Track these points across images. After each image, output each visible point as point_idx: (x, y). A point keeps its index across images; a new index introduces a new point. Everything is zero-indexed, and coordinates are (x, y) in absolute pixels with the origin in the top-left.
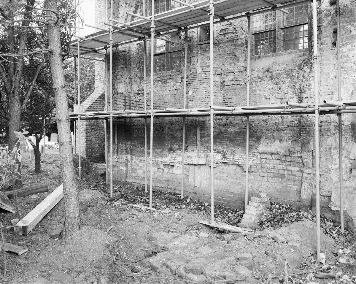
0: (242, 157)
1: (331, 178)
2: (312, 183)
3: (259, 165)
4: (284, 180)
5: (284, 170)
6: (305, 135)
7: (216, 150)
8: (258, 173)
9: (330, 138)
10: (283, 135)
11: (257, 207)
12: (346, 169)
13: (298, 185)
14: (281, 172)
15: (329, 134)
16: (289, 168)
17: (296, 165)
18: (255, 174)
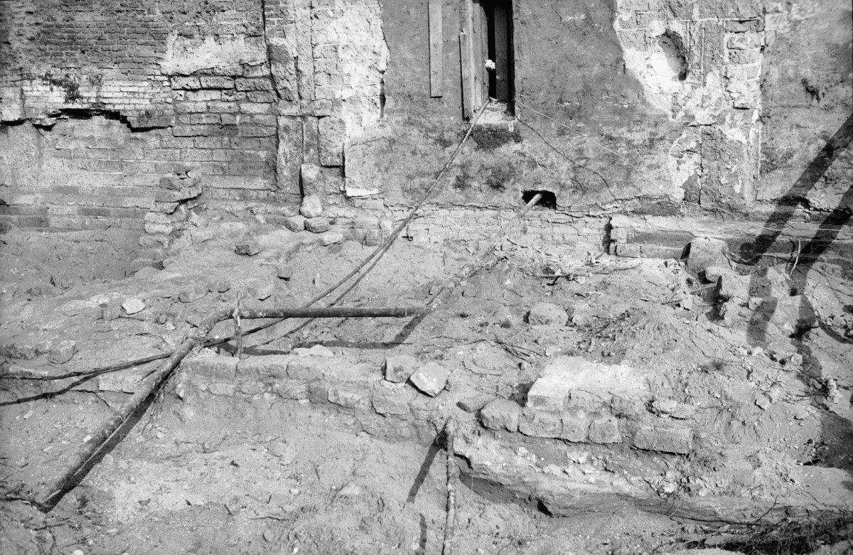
0: (123, 89)
1: (341, 122)
2: (300, 138)
3: (169, 106)
4: (236, 139)
5: (234, 114)
6: (275, 20)
7: (49, 78)
8: (169, 128)
9: (334, 23)
10: (224, 23)
11: (171, 214)
12: (373, 98)
13: (267, 149)
14: (227, 119)
15: (331, 13)
16: (245, 107)
17: (261, 98)
18: (160, 131)
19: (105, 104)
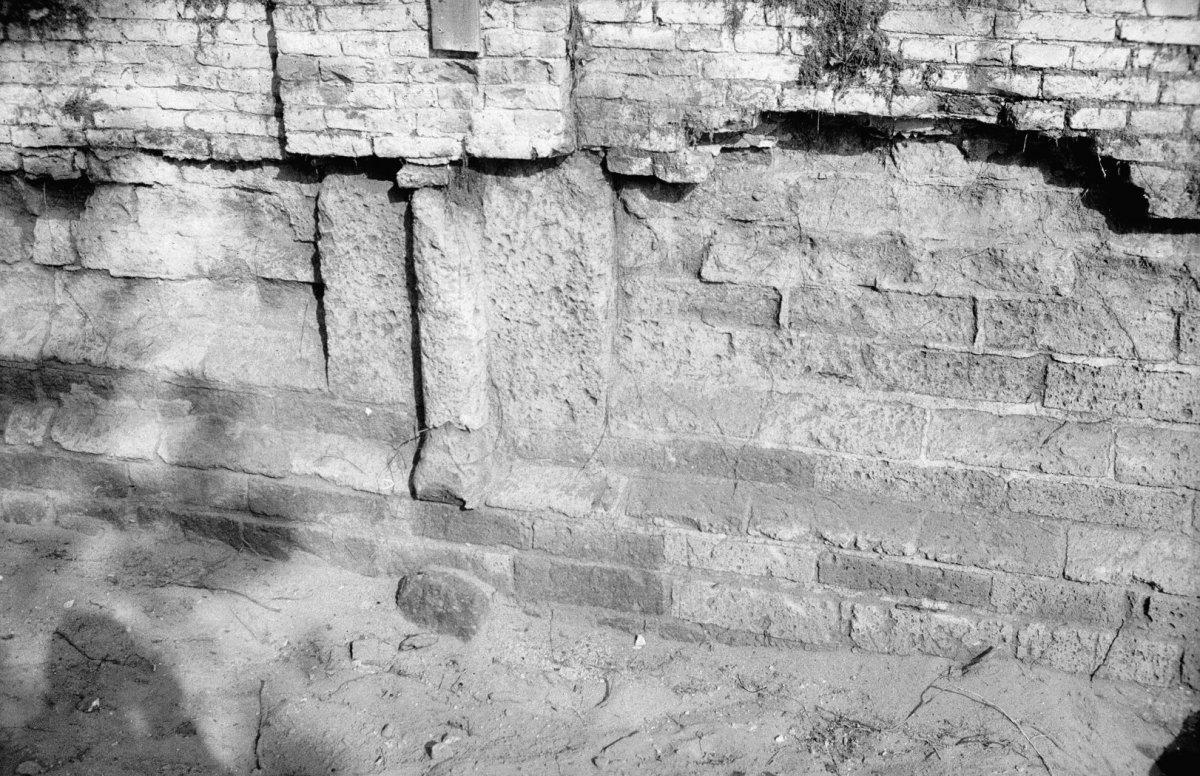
0: (1131, 31)
19: (1019, 98)
